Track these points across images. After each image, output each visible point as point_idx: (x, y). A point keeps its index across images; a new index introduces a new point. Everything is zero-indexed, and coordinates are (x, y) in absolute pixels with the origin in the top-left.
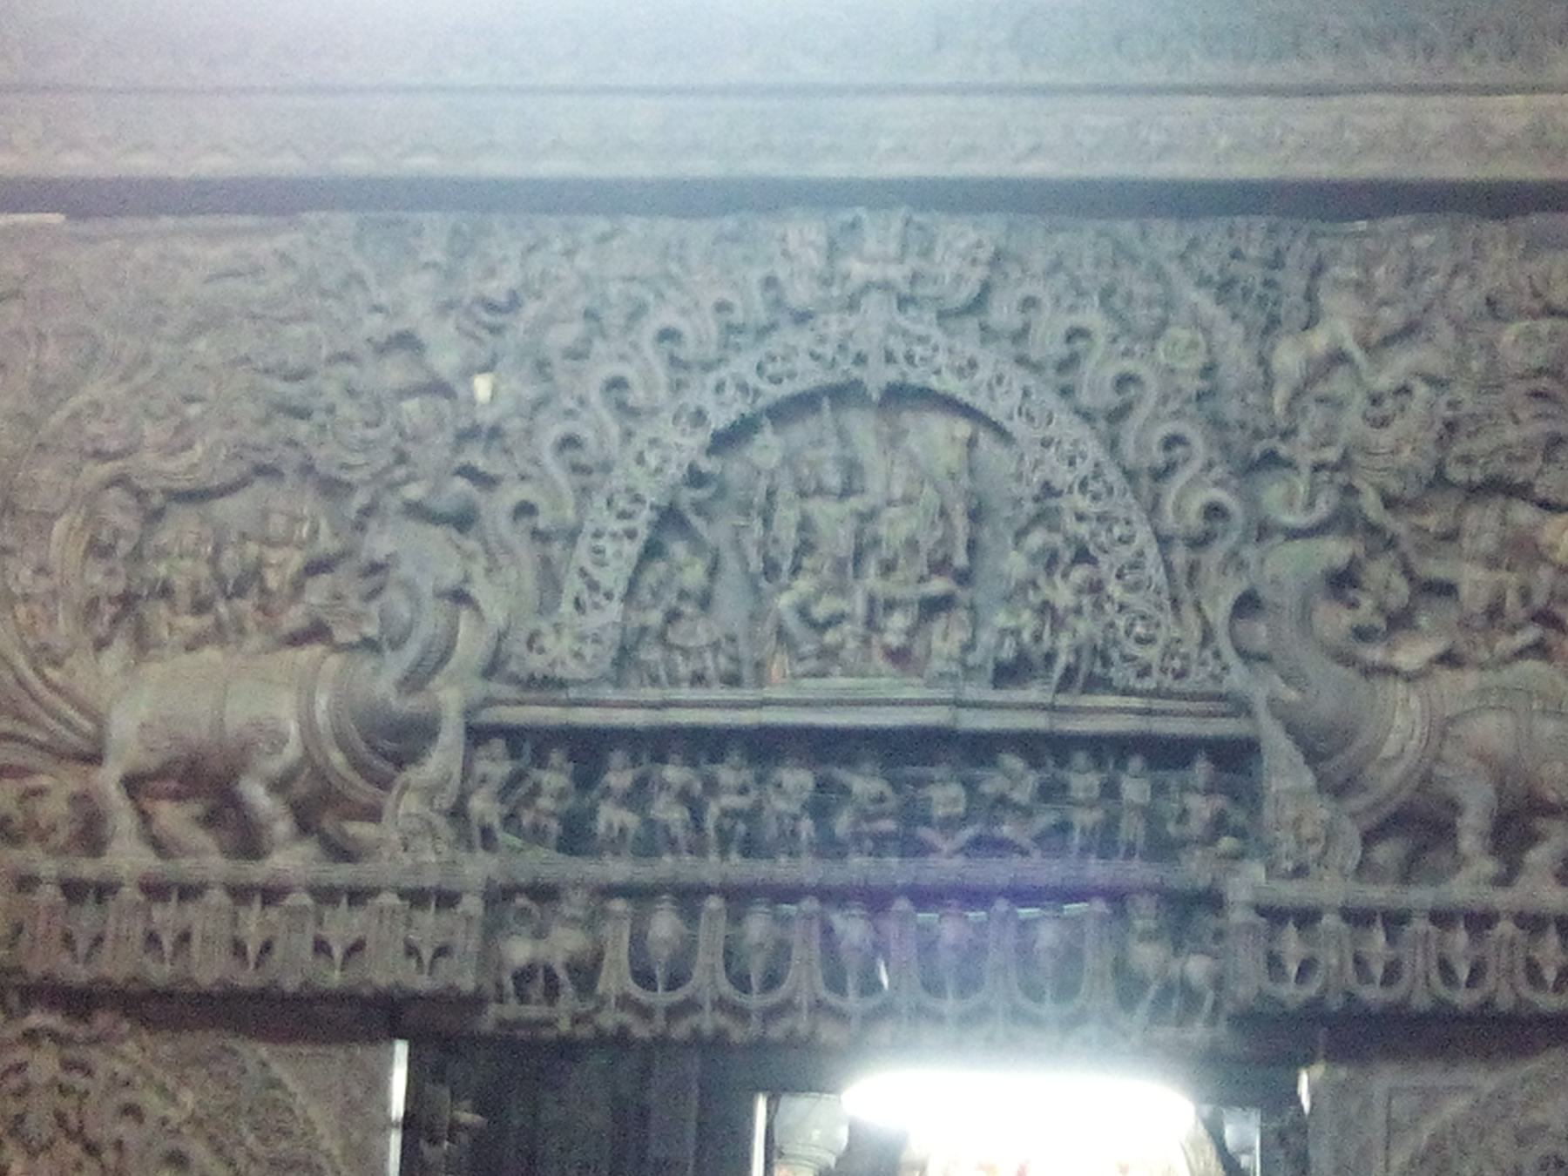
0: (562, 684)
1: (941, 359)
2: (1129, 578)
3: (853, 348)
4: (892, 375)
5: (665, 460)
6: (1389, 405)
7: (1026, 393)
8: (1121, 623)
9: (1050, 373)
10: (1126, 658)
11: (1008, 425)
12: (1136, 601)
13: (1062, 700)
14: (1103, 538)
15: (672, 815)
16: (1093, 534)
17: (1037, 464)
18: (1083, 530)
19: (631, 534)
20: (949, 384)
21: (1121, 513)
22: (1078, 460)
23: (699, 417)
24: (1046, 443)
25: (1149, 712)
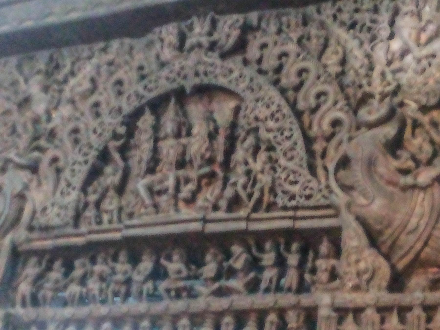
0: (53, 228)
1: (218, 71)
2: (289, 155)
3: (183, 73)
4: (197, 81)
5: (104, 130)
6: (424, 63)
7: (252, 80)
8: (283, 176)
9: (271, 74)
10: (285, 192)
11: (242, 95)
12: (291, 165)
13: (254, 215)
14: (279, 138)
15: (94, 285)
16: (275, 137)
17: (253, 109)
18: (270, 136)
19: (86, 162)
20: (222, 81)
21: (287, 125)
22: (271, 105)
23: (120, 110)
24: (257, 100)
25: (294, 218)
